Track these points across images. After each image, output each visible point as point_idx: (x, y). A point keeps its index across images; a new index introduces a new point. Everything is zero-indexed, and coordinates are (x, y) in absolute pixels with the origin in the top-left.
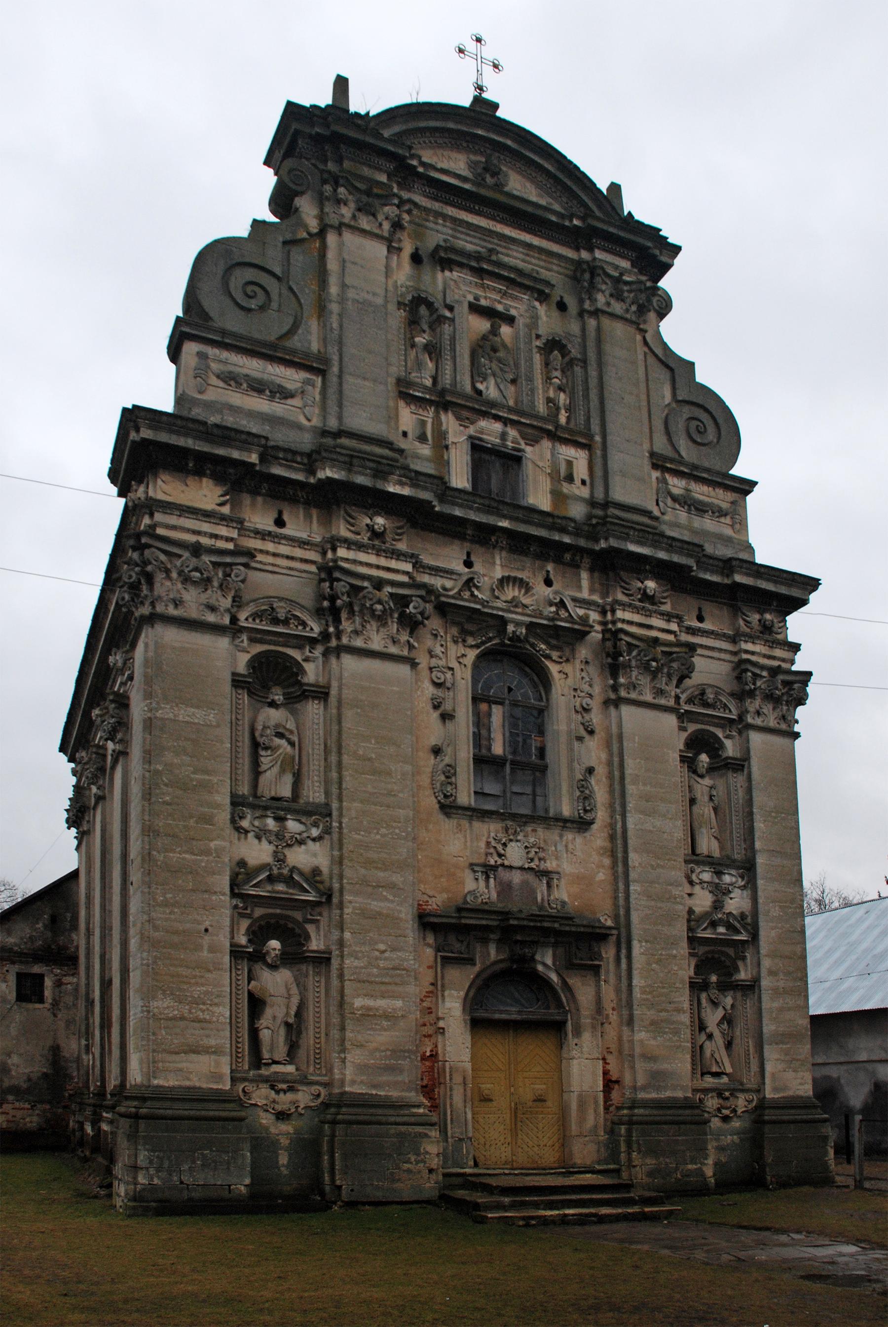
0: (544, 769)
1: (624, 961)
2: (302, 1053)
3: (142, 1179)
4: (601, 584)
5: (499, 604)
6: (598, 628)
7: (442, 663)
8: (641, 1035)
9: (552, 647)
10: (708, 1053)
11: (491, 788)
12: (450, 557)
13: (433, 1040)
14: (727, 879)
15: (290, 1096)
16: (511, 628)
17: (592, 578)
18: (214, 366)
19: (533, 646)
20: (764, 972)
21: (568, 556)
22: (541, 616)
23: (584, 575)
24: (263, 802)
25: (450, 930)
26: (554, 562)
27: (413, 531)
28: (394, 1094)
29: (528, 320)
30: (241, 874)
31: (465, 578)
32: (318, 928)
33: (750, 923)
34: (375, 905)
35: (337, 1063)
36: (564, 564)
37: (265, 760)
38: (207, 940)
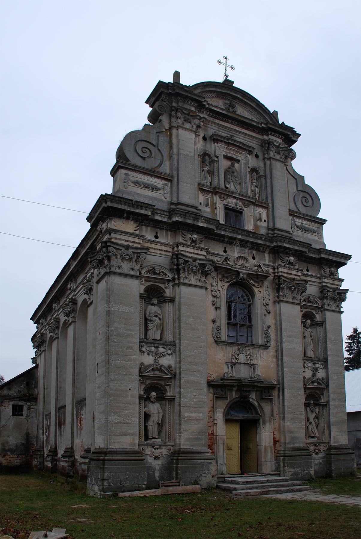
0: (251, 327)
1: (281, 397)
2: (163, 434)
3: (106, 484)
4: (272, 258)
5: (237, 266)
6: (272, 275)
7: (216, 288)
8: (288, 424)
9: (255, 282)
10: (310, 429)
11: (233, 334)
12: (218, 249)
13: (212, 427)
14: (317, 365)
15: (160, 450)
16: (241, 275)
17: (269, 257)
18: (131, 178)
19: (248, 281)
20: (331, 399)
21: (261, 248)
22: (252, 270)
23: (267, 255)
24: (150, 341)
25: (218, 387)
26: (256, 250)
28: (199, 448)
29: (245, 161)
30: (142, 367)
31: (225, 257)
32: (170, 387)
33: (326, 382)
34: (192, 379)
35: (178, 438)
36: (259, 251)
37: (150, 325)
38: (130, 393)
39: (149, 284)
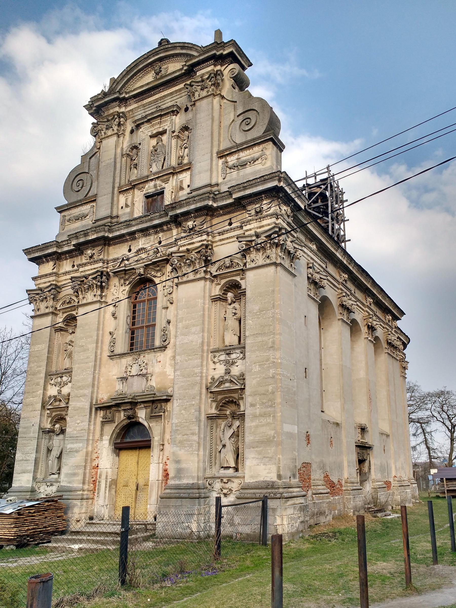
9: (158, 271)
21: (165, 228)
27: (111, 248)
34: (79, 405)
39: (65, 315)
